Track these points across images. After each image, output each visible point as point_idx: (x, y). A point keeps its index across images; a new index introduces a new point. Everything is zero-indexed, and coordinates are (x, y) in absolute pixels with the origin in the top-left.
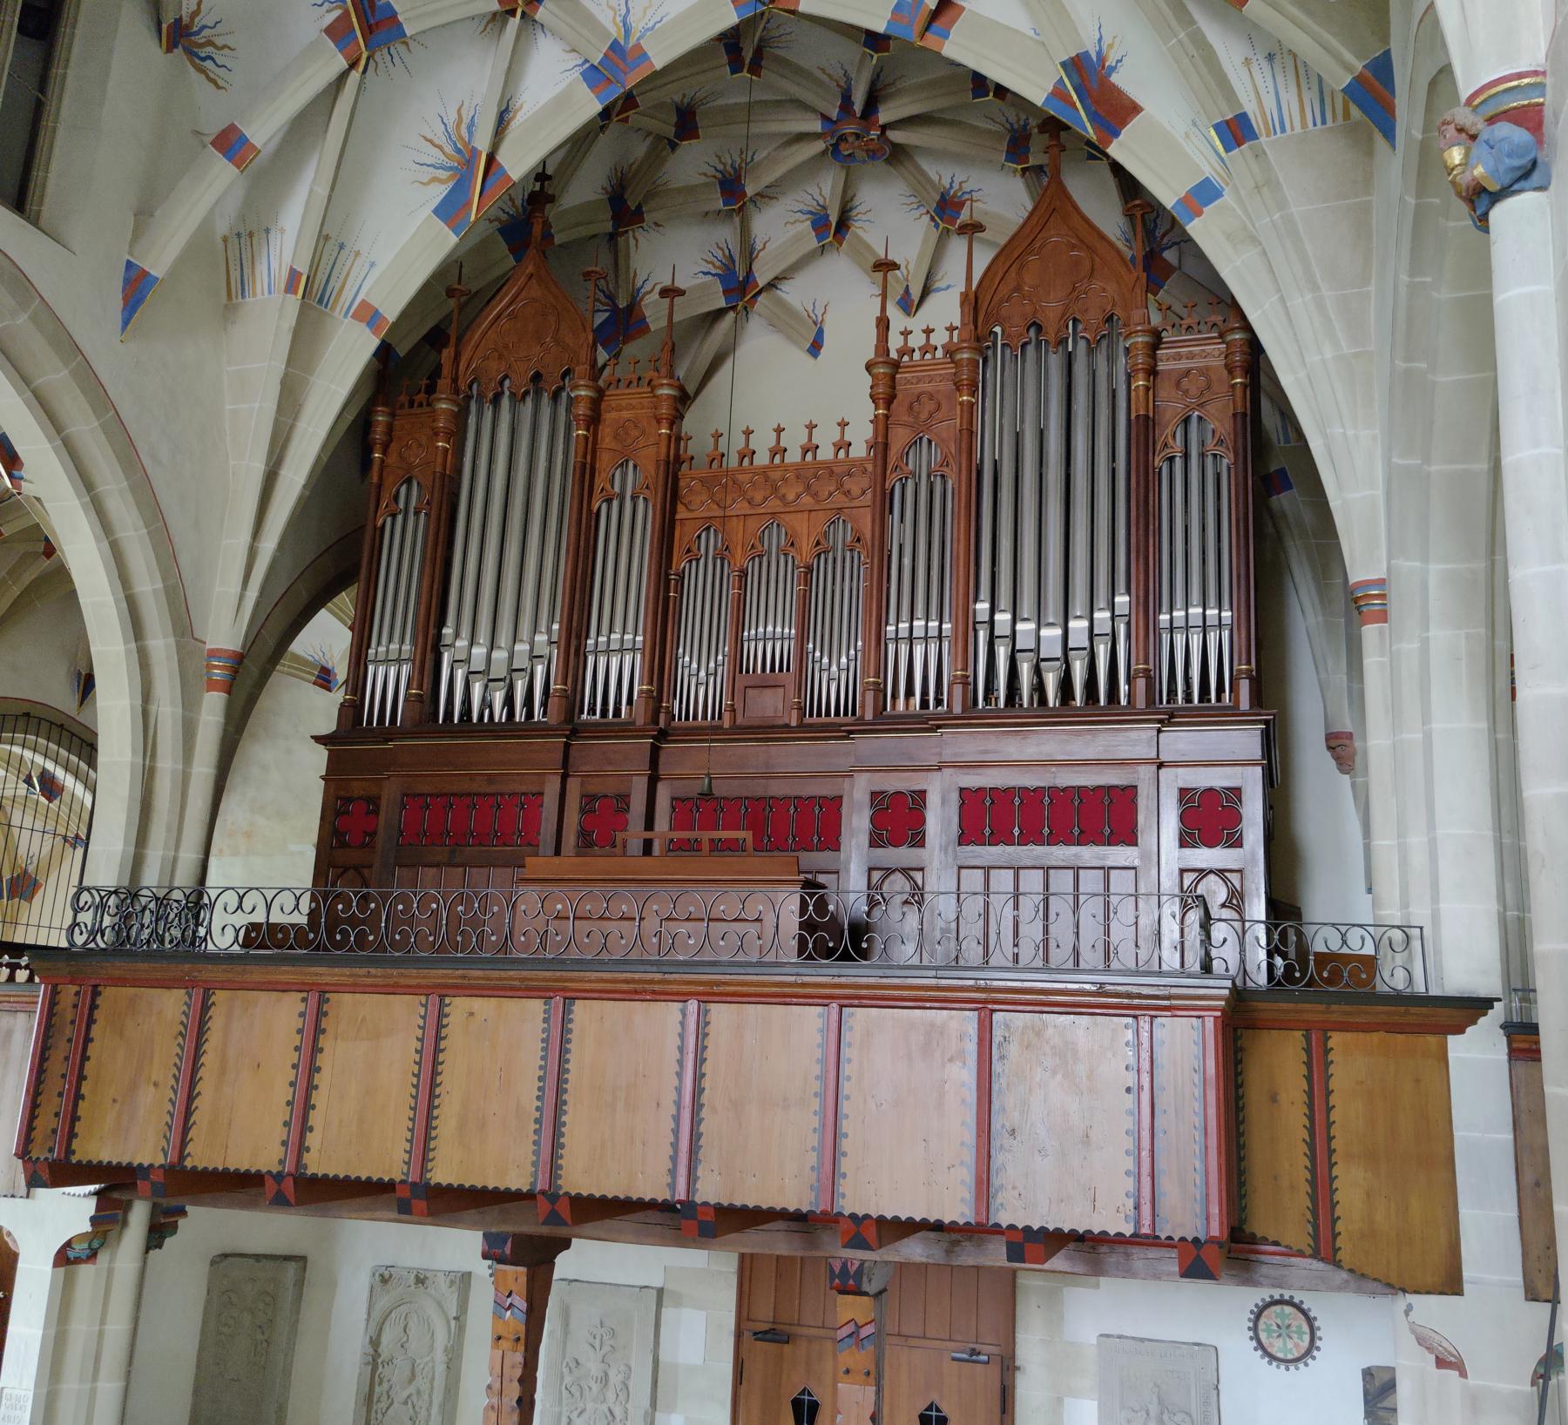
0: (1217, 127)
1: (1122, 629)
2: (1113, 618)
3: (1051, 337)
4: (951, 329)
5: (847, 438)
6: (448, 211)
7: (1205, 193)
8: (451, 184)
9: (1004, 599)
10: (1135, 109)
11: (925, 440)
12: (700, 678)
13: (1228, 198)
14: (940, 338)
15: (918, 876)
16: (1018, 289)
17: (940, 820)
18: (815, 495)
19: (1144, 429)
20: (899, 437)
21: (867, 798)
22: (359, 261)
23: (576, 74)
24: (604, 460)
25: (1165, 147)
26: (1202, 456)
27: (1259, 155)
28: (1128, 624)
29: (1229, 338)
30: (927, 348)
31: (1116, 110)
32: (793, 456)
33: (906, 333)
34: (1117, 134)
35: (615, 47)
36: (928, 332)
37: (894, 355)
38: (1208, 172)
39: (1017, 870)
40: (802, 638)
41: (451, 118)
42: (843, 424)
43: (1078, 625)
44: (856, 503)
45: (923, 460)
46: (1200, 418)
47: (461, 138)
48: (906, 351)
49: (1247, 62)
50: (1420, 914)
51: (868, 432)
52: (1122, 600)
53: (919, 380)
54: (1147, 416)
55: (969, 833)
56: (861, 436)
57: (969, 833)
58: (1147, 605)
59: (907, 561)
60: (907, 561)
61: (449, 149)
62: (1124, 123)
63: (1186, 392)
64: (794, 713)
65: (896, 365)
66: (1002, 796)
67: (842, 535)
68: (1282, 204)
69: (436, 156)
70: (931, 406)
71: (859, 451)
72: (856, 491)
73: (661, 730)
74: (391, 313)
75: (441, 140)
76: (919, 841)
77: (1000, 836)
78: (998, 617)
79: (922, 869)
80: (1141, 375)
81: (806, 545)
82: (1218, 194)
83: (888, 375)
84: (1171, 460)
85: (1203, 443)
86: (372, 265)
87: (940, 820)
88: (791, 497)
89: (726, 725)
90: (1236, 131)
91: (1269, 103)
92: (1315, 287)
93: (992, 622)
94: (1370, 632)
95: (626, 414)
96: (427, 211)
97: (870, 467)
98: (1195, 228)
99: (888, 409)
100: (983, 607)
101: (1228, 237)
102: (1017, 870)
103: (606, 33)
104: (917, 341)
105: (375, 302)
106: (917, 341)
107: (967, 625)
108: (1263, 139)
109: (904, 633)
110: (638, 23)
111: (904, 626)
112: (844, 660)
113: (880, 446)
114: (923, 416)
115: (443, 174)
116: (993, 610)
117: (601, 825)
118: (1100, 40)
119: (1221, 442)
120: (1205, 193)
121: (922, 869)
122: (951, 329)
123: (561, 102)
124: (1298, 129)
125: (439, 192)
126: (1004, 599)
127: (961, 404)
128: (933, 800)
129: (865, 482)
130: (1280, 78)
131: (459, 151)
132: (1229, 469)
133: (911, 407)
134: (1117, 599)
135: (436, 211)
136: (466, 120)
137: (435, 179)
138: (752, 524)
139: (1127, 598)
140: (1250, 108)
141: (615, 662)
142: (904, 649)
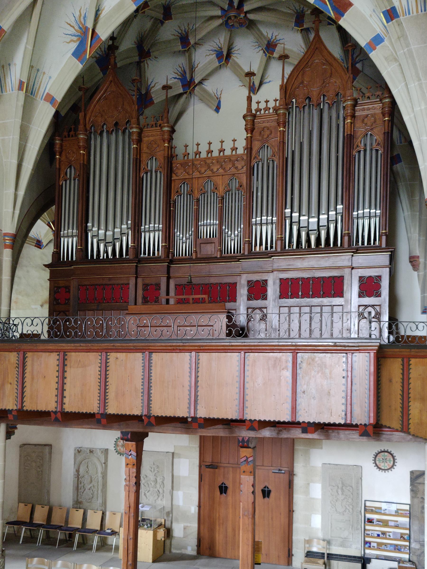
0: (383, 13)
1: (339, 218)
2: (336, 214)
3: (315, 103)
4: (276, 100)
5: (236, 146)
6: (78, 54)
7: (377, 40)
8: (78, 43)
9: (296, 208)
11: (266, 146)
13: (386, 42)
14: (271, 104)
15: (265, 310)
16: (302, 82)
17: (273, 290)
18: (224, 169)
19: (350, 140)
20: (256, 145)
21: (246, 283)
22: (45, 76)
24: (144, 157)
25: (362, 21)
26: (371, 150)
27: (400, 24)
28: (342, 216)
29: (384, 101)
33: (258, 103)
34: (343, 15)
36: (267, 102)
37: (254, 112)
38: (379, 31)
39: (300, 307)
40: (221, 225)
41: (77, 14)
42: (234, 141)
43: (323, 217)
44: (240, 172)
45: (266, 154)
46: (371, 135)
47: (81, 23)
51: (244, 143)
52: (340, 207)
53: (264, 122)
54: (351, 135)
55: (283, 295)
56: (241, 145)
57: (283, 295)
58: (349, 209)
59: (259, 194)
60: (259, 194)
61: (77, 28)
62: (346, 10)
63: (366, 124)
64: (219, 253)
65: (254, 116)
66: (295, 281)
67: (235, 184)
68: (408, 45)
69: (72, 31)
70: (268, 132)
71: (240, 151)
72: (240, 167)
73: (170, 259)
74: (59, 97)
75: (74, 24)
76: (265, 298)
77: (295, 295)
78: (293, 215)
79: (266, 308)
80: (349, 118)
81: (221, 188)
83: (251, 119)
84: (359, 152)
85: (371, 144)
86: (50, 78)
87: (273, 290)
88: (215, 170)
89: (194, 257)
92: (419, 80)
93: (291, 217)
95: (151, 138)
97: (245, 158)
98: (373, 55)
99: (252, 134)
100: (288, 211)
102: (300, 307)
104: (262, 106)
105: (52, 93)
106: (262, 106)
107: (282, 218)
109: (258, 222)
111: (258, 219)
112: (236, 232)
113: (249, 148)
114: (265, 136)
115: (75, 38)
116: (292, 212)
119: (379, 144)
120: (377, 40)
121: (266, 308)
122: (276, 100)
125: (74, 46)
126: (296, 208)
127: (280, 131)
128: (270, 283)
129: (243, 163)
131: (80, 28)
132: (381, 155)
133: (260, 133)
134: (338, 207)
136: (83, 15)
137: (72, 41)
138: (201, 181)
139: (341, 206)
140: (396, 4)
141: (152, 235)
142: (259, 227)
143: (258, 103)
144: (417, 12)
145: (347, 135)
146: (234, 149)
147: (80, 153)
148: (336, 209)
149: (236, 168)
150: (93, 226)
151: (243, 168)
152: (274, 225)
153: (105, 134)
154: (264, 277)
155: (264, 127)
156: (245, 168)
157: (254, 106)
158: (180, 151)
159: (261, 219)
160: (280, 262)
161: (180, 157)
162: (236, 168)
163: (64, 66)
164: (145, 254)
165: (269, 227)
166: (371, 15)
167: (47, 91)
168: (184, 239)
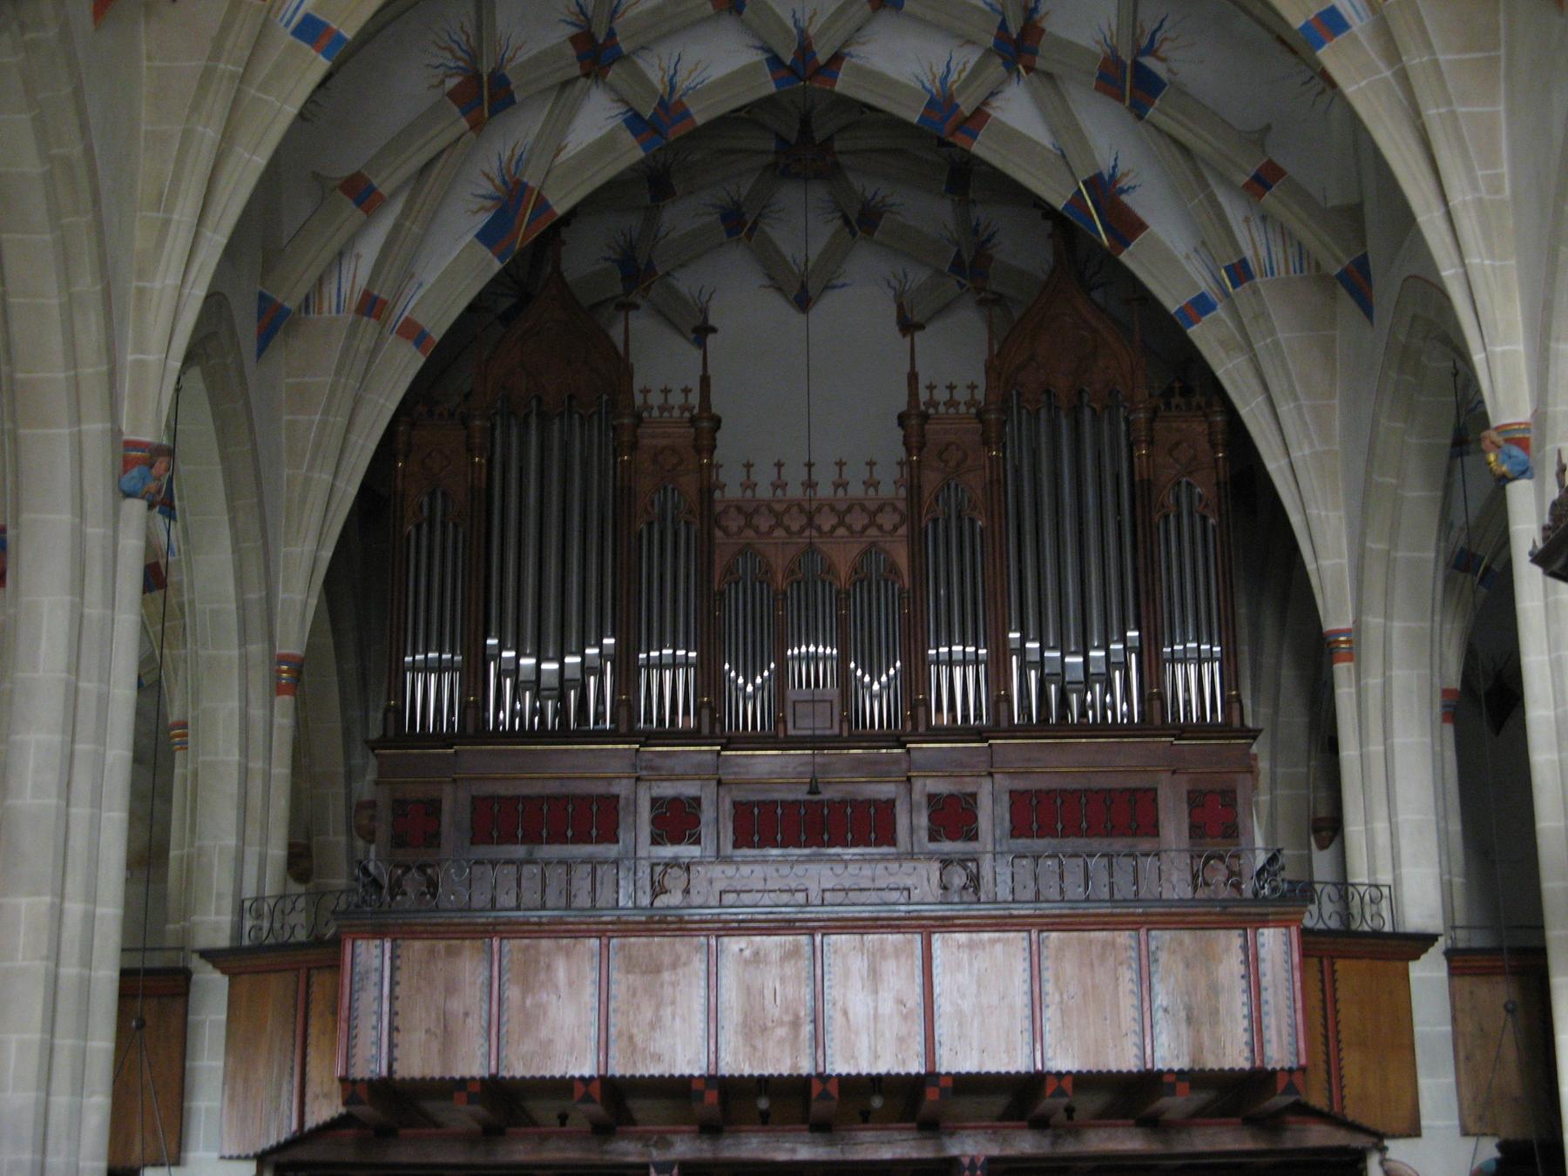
4: (973, 387)
5: (876, 476)
7: (1202, 305)
10: (1142, 226)
12: (747, 690)
13: (1221, 311)
14: (962, 395)
17: (991, 815)
19: (1142, 493)
20: (931, 480)
21: (924, 801)
23: (619, 120)
27: (1256, 291)
30: (951, 403)
31: (1127, 227)
32: (825, 491)
33: (931, 388)
34: (1127, 245)
35: (662, 104)
36: (951, 388)
37: (923, 408)
38: (1203, 287)
40: (843, 660)
46: (1188, 484)
47: (509, 170)
48: (932, 403)
49: (1247, 220)
50: (1385, 877)
52: (1133, 634)
55: (1019, 829)
57: (1019, 829)
61: (498, 181)
62: (1134, 237)
65: (925, 417)
69: (487, 188)
71: (887, 490)
72: (888, 526)
75: (495, 173)
81: (844, 571)
82: (1212, 307)
86: (421, 285)
87: (991, 815)
88: (826, 528)
90: (1240, 272)
91: (1263, 253)
94: (1342, 670)
95: (663, 442)
96: (470, 237)
97: (901, 505)
99: (919, 455)
101: (1222, 344)
103: (655, 91)
104: (942, 395)
105: (421, 320)
106: (942, 395)
108: (1258, 279)
110: (683, 82)
112: (884, 679)
113: (914, 490)
114: (952, 463)
115: (489, 203)
116: (1023, 640)
117: (676, 821)
118: (1114, 167)
120: (1202, 305)
122: (973, 387)
123: (603, 147)
124: (1283, 274)
125: (483, 219)
127: (991, 458)
129: (897, 518)
130: (1271, 236)
131: (504, 182)
134: (1130, 634)
135: (478, 236)
137: (482, 209)
139: (1136, 634)
140: (1248, 253)
142: (944, 670)
143: (931, 388)
144: (1287, 272)
145: (1141, 481)
146: (872, 484)
147: (473, 463)
148: (1124, 639)
149: (880, 528)
150: (502, 646)
151: (895, 528)
152: (982, 668)
153: (533, 421)
155: (948, 445)
156: (903, 530)
157: (924, 395)
159: (950, 651)
161: (733, 492)
162: (880, 528)
163: (455, 260)
164: (648, 719)
165: (971, 671)
166: (1187, 257)
167: (406, 313)
168: (750, 688)
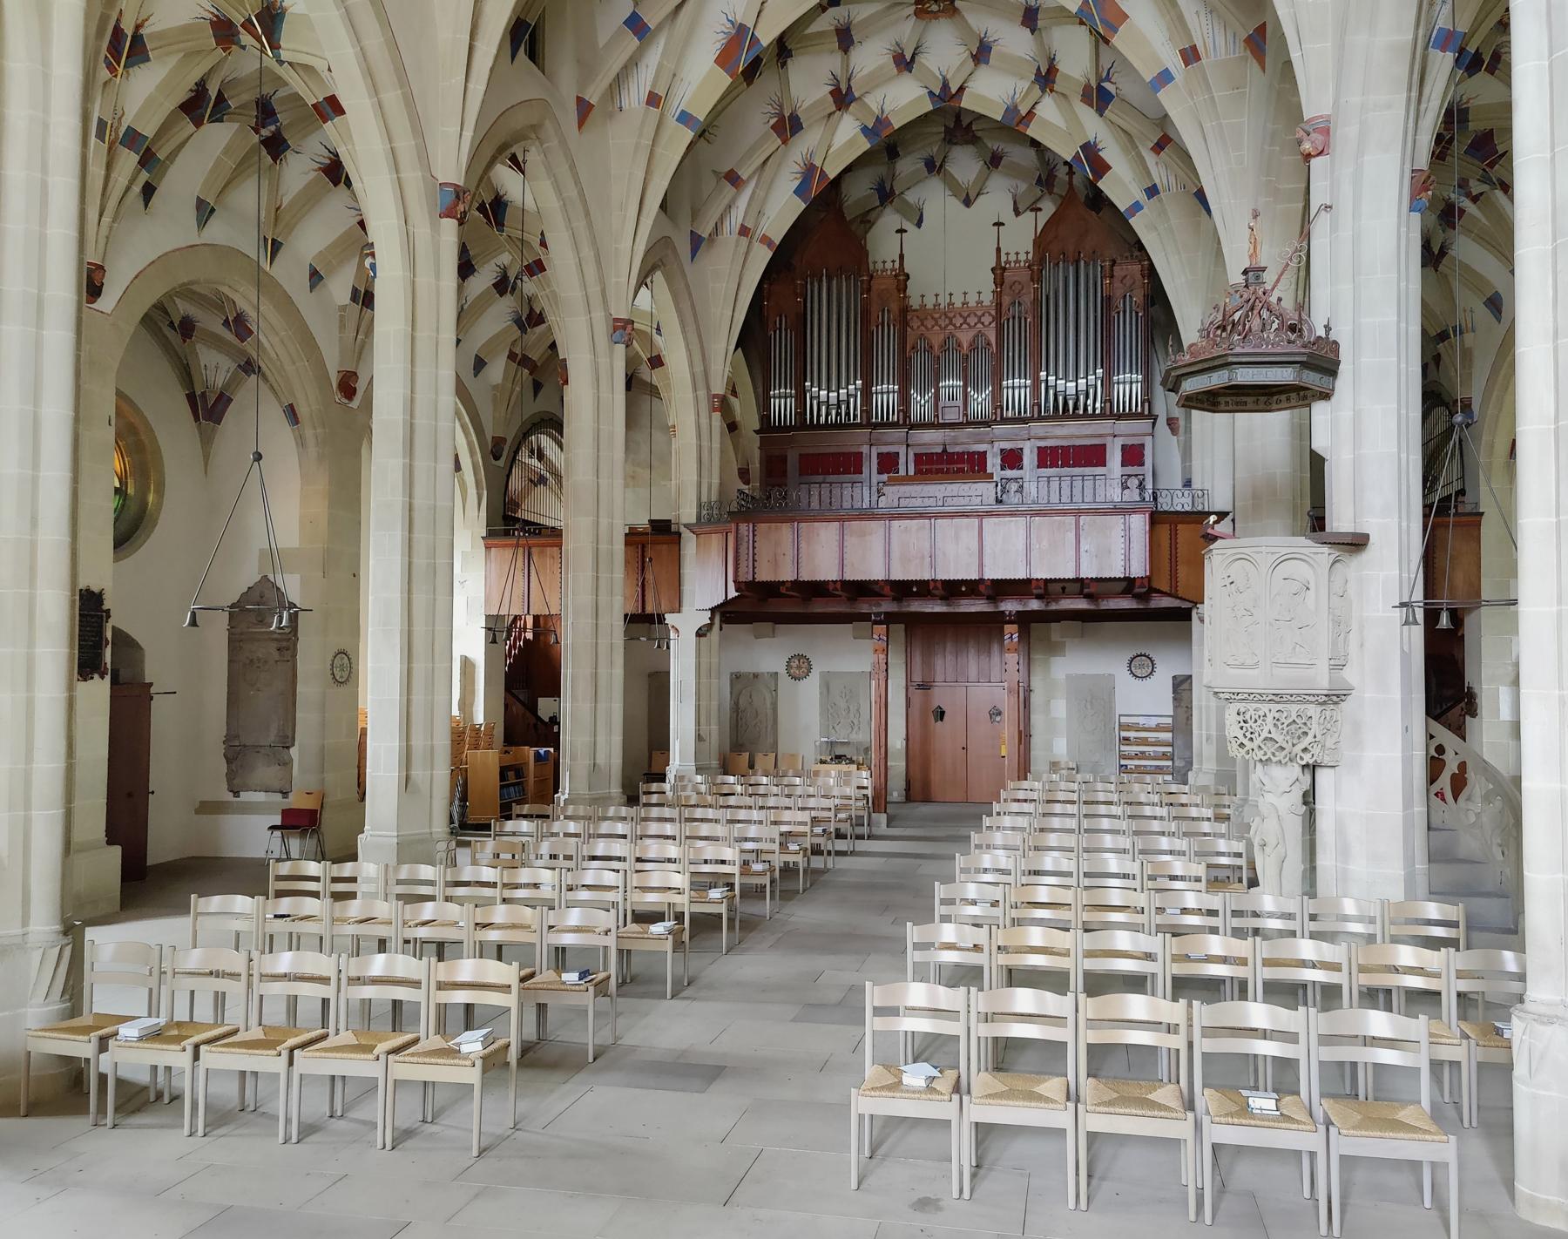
7: (1136, 207)
12: (921, 403)
13: (1146, 210)
14: (1022, 257)
17: (1029, 458)
19: (1108, 301)
20: (1006, 300)
27: (1160, 200)
30: (1017, 261)
31: (1101, 168)
40: (965, 386)
48: (1008, 262)
52: (1099, 371)
55: (1041, 464)
56: (988, 298)
57: (1041, 464)
65: (1004, 269)
66: (1054, 449)
69: (797, 169)
77: (1054, 465)
87: (1029, 458)
90: (1152, 191)
100: (1043, 374)
104: (1012, 258)
106: (1012, 258)
107: (1036, 382)
110: (887, 109)
113: (999, 306)
120: (1136, 207)
123: (851, 143)
125: (797, 183)
140: (1157, 181)
154: (1019, 445)
157: (1004, 258)
158: (915, 302)
160: (1037, 428)
